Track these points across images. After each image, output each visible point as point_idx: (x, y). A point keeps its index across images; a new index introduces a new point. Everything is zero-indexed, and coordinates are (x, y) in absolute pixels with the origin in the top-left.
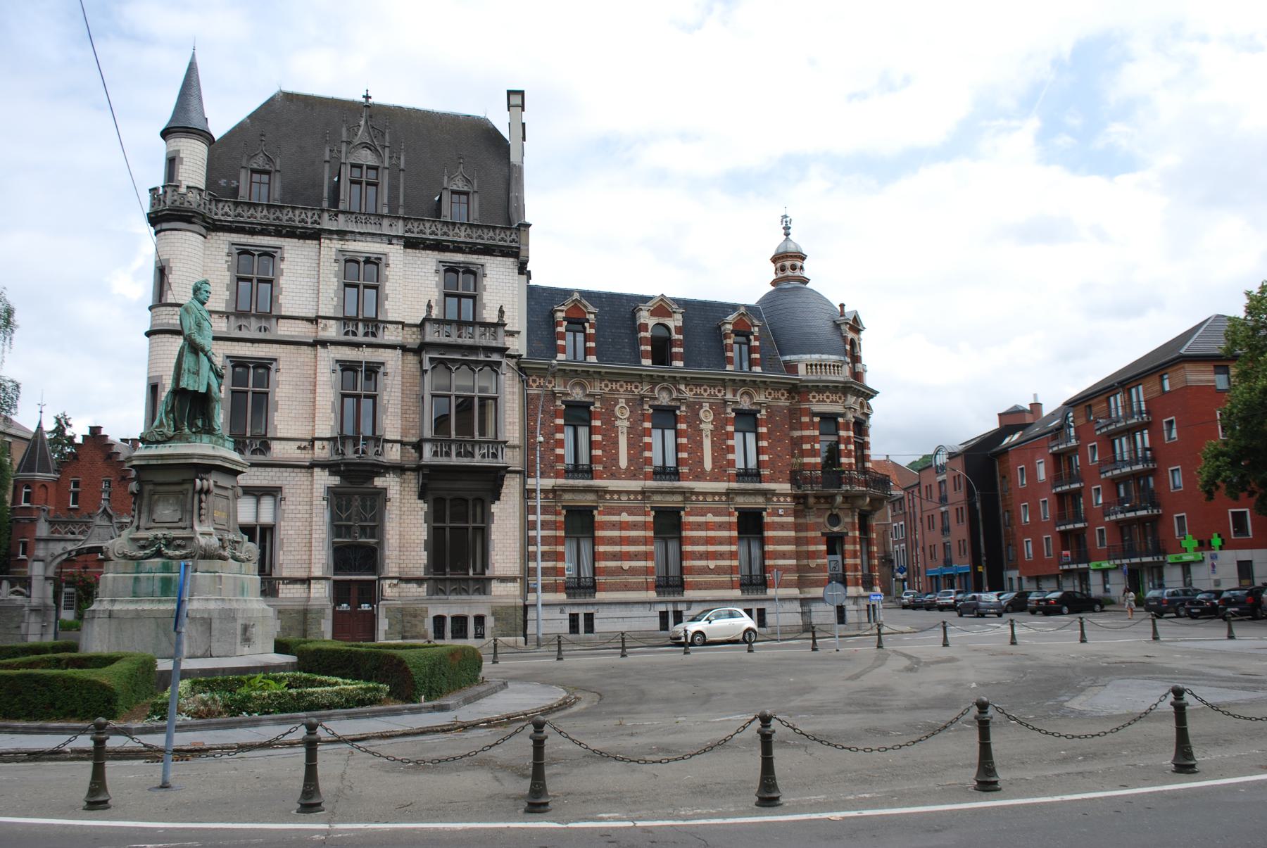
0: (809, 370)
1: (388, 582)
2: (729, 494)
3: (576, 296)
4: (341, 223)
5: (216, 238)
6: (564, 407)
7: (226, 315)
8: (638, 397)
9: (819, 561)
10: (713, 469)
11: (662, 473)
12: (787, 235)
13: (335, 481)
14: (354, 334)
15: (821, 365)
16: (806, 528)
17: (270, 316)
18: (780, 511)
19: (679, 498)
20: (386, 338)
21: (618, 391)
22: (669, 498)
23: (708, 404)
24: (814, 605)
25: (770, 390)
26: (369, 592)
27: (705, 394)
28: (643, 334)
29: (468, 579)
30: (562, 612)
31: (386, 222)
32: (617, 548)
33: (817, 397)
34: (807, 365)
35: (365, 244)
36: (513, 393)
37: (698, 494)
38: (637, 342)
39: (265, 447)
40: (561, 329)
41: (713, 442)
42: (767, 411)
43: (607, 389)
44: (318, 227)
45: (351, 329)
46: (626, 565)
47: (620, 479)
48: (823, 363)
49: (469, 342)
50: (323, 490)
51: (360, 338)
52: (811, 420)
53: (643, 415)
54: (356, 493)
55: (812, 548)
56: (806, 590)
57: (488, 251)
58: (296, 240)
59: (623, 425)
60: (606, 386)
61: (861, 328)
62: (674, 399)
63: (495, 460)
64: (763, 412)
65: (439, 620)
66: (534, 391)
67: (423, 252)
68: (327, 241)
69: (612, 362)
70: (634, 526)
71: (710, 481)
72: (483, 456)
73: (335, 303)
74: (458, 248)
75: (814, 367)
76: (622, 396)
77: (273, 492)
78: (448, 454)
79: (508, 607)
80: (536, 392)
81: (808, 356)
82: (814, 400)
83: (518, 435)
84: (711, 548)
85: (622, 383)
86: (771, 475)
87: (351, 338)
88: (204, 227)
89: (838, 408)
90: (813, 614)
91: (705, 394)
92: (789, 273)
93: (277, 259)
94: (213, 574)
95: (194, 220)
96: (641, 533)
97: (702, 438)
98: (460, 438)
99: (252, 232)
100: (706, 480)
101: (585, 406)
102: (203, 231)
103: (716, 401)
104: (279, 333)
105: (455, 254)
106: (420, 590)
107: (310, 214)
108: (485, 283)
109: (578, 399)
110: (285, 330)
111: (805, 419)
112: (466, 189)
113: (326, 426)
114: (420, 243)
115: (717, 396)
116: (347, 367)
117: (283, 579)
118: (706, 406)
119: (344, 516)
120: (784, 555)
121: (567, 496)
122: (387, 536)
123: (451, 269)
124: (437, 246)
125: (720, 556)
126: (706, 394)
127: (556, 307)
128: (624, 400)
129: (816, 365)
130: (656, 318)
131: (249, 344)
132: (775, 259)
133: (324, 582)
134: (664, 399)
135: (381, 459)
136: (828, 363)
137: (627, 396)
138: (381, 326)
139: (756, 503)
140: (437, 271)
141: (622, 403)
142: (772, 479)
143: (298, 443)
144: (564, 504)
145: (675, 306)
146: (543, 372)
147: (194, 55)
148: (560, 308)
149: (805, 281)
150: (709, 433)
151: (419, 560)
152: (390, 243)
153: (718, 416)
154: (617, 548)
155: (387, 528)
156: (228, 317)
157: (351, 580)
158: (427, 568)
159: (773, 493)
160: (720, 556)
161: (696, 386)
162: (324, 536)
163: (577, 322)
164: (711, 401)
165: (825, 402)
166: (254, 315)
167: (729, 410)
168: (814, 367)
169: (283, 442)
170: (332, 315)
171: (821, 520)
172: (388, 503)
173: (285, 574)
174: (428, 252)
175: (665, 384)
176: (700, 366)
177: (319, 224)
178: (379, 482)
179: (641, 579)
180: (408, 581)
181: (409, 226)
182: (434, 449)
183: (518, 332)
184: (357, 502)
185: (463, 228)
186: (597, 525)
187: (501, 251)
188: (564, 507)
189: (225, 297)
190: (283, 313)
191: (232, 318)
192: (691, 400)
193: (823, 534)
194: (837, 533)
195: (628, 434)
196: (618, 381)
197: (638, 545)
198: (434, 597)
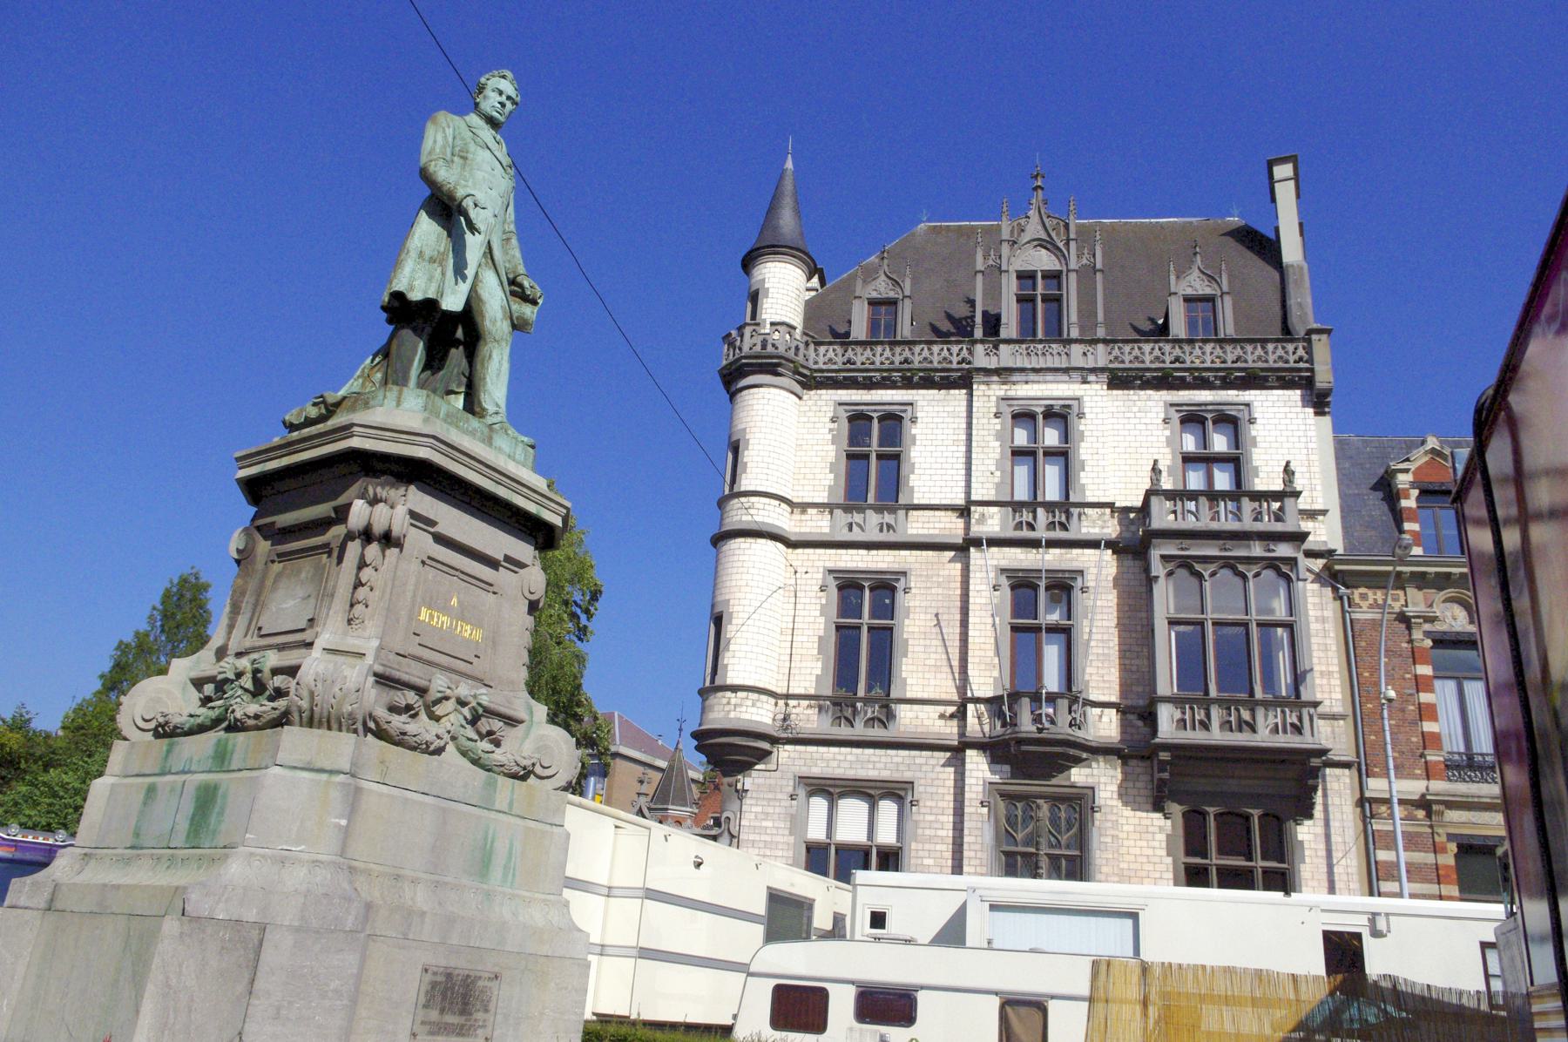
5: (816, 397)
6: (1429, 643)
7: (829, 507)
14: (1031, 527)
20: (1084, 530)
31: (1076, 349)
35: (1043, 386)
36: (1323, 620)
45: (1024, 519)
50: (980, 789)
51: (1041, 533)
57: (1253, 380)
66: (1364, 614)
67: (1142, 392)
68: (983, 387)
73: (997, 480)
77: (898, 792)
83: (1339, 696)
87: (1026, 533)
88: (798, 382)
93: (906, 422)
94: (324, 777)
99: (869, 385)
102: (798, 388)
104: (910, 531)
108: (1253, 433)
110: (918, 526)
112: (1208, 291)
113: (986, 680)
114: (1136, 378)
121: (1453, 815)
124: (1163, 381)
127: (1394, 466)
135: (1080, 734)
138: (1075, 511)
143: (941, 709)
144: (1452, 831)
152: (1085, 382)
155: (1098, 862)
156: (831, 513)
169: (916, 707)
170: (992, 498)
172: (1097, 815)
177: (969, 363)
178: (1078, 775)
181: (1116, 352)
182: (1178, 715)
183: (1324, 512)
187: (1279, 378)
188: (1451, 837)
189: (827, 483)
190: (916, 502)
191: (838, 512)
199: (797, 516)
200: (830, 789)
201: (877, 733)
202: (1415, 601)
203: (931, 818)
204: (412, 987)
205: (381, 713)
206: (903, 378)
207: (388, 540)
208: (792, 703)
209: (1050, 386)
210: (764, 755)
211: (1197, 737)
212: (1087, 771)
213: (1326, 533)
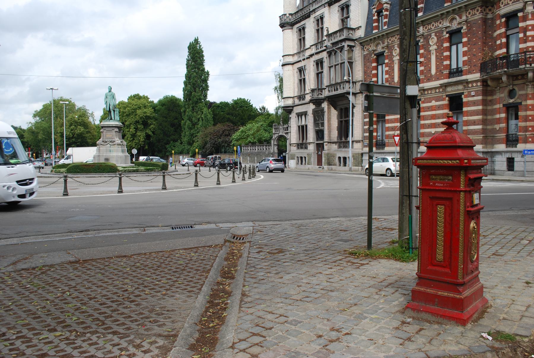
2: (445, 86)
6: (375, 57)
10: (436, 73)
24: (497, 156)
25: (470, 11)
29: (342, 142)
41: (436, 56)
42: (467, 27)
43: (390, 42)
64: (465, 27)
65: (340, 158)
71: (435, 81)
79: (357, 154)
86: (469, 69)
97: (431, 56)
100: (432, 81)
102: (290, 27)
103: (438, 30)
109: (380, 51)
118: (433, 35)
120: (474, 123)
126: (433, 27)
135: (320, 96)
139: (458, 90)
142: (469, 72)
148: (373, 7)
153: (439, 39)
159: (467, 82)
165: (509, 4)
167: (445, 33)
171: (502, 95)
180: (333, 143)
183: (360, 27)
192: (426, 34)
193: (504, 105)
194: (513, 103)
204: (104, 159)
213: (361, 33)
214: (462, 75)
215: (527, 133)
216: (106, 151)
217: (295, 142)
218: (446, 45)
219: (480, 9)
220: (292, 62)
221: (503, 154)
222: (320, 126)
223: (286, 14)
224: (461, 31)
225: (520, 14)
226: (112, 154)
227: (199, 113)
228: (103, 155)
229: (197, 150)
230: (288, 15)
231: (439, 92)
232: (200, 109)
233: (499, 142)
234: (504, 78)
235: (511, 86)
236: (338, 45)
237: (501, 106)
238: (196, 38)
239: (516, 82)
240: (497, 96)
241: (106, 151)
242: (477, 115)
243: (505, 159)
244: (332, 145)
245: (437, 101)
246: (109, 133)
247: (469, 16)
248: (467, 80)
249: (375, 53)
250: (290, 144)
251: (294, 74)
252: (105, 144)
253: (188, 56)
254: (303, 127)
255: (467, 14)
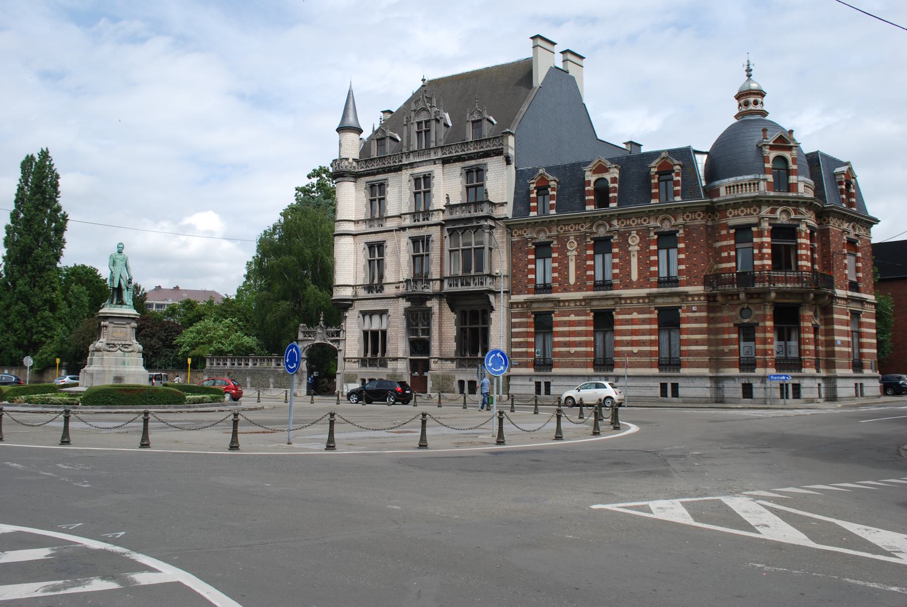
0: (728, 191)
1: (433, 360)
3: (663, 155)
4: (412, 159)
6: (534, 247)
8: (583, 234)
9: (732, 347)
10: (639, 279)
11: (606, 285)
12: (749, 76)
13: (408, 304)
14: (419, 221)
15: (737, 186)
16: (723, 320)
17: (383, 218)
18: (693, 308)
19: (611, 302)
21: (570, 231)
22: (604, 303)
23: (635, 232)
24: (726, 382)
25: (688, 214)
26: (426, 366)
27: (634, 224)
28: (587, 188)
30: (530, 380)
32: (567, 339)
33: (745, 211)
34: (726, 187)
36: (503, 242)
37: (626, 299)
38: (584, 193)
39: (381, 288)
40: (534, 195)
41: (639, 259)
42: (684, 231)
43: (562, 231)
44: (401, 163)
46: (573, 350)
47: (570, 291)
48: (739, 184)
49: (467, 215)
50: (403, 310)
51: (421, 223)
52: (728, 232)
53: (586, 245)
54: (419, 311)
55: (726, 336)
56: (722, 370)
57: (487, 154)
58: (393, 173)
59: (572, 254)
60: (561, 229)
61: (792, 144)
62: (608, 232)
63: (481, 286)
64: (681, 231)
65: (461, 383)
66: (515, 239)
69: (566, 211)
70: (579, 323)
71: (636, 288)
72: (476, 285)
74: (470, 157)
75: (732, 188)
76: (572, 234)
77: (382, 313)
78: (457, 285)
80: (516, 239)
81: (726, 180)
82: (731, 216)
83: (506, 269)
84: (635, 338)
85: (572, 225)
86: (687, 280)
87: (417, 223)
89: (753, 220)
90: (726, 389)
91: (634, 224)
92: (752, 107)
95: (345, 175)
96: (584, 328)
97: (630, 257)
98: (465, 274)
99: (373, 174)
100: (633, 288)
101: (547, 245)
103: (642, 228)
104: (387, 226)
105: (470, 161)
106: (453, 365)
107: (397, 158)
109: (543, 241)
110: (390, 224)
111: (724, 232)
112: (479, 118)
113: (406, 273)
115: (643, 224)
116: (415, 241)
117: (390, 358)
118: (634, 233)
119: (414, 324)
120: (696, 342)
122: (433, 334)
123: (468, 172)
124: (459, 159)
125: (643, 343)
126: (634, 224)
128: (573, 237)
129: (734, 186)
130: (597, 175)
131: (374, 235)
132: (738, 97)
133: (403, 360)
134: (602, 232)
135: (426, 290)
136: (743, 183)
137: (575, 234)
139: (673, 303)
140: (461, 174)
141: (572, 239)
142: (688, 283)
143: (396, 285)
145: (609, 163)
146: (521, 226)
147: (351, 86)
148: (531, 182)
149: (764, 113)
150: (574, 258)
151: (451, 347)
152: (435, 164)
153: (643, 239)
154: (567, 339)
155: (433, 330)
157: (417, 359)
158: (456, 352)
159: (686, 294)
160: (643, 343)
161: (626, 219)
162: (403, 335)
163: (542, 189)
164: (638, 228)
165: (740, 216)
166: (376, 219)
167: (652, 234)
168: (732, 188)
170: (407, 212)
171: (733, 313)
173: (390, 356)
174: (456, 163)
175: (601, 222)
176: (630, 204)
178: (429, 304)
179: (583, 359)
180: (446, 360)
181: (444, 151)
183: (506, 203)
184: (420, 315)
185: (472, 145)
186: (533, 325)
187: (494, 153)
188: (533, 313)
190: (389, 215)
191: (367, 222)
192: (622, 230)
193: (735, 325)
194: (748, 323)
195: (576, 260)
196: (569, 224)
197: (582, 336)
198: (459, 369)
199: (356, 225)
200: (371, 313)
201: (379, 295)
202: (529, 234)
203: (393, 320)
204: (112, 378)
205: (108, 349)
206: (383, 171)
207: (106, 327)
208: (357, 287)
209: (425, 167)
210: (351, 305)
211: (454, 289)
212: (430, 302)
213: (507, 212)
214: (678, 286)
215: (767, 357)
216: (116, 363)
217: (357, 357)
218: (654, 247)
219: (702, 215)
220: (352, 231)
221: (737, 379)
222: (420, 334)
223: (348, 159)
224: (675, 234)
225: (754, 229)
226: (127, 369)
227: (47, 288)
228: (110, 371)
229: (58, 361)
230: (351, 160)
231: (644, 302)
232: (48, 282)
233: (730, 365)
234: (742, 296)
235: (746, 305)
236: (472, 222)
237: (731, 325)
238: (45, 150)
239: (751, 301)
240: (725, 313)
241: (116, 363)
242: (701, 334)
243: (740, 386)
244: (447, 362)
245: (639, 313)
246: (119, 330)
247: (688, 219)
248: (687, 292)
249: (533, 241)
250: (345, 359)
251: (356, 253)
252: (111, 349)
253: (20, 180)
254: (375, 333)
255: (685, 217)
